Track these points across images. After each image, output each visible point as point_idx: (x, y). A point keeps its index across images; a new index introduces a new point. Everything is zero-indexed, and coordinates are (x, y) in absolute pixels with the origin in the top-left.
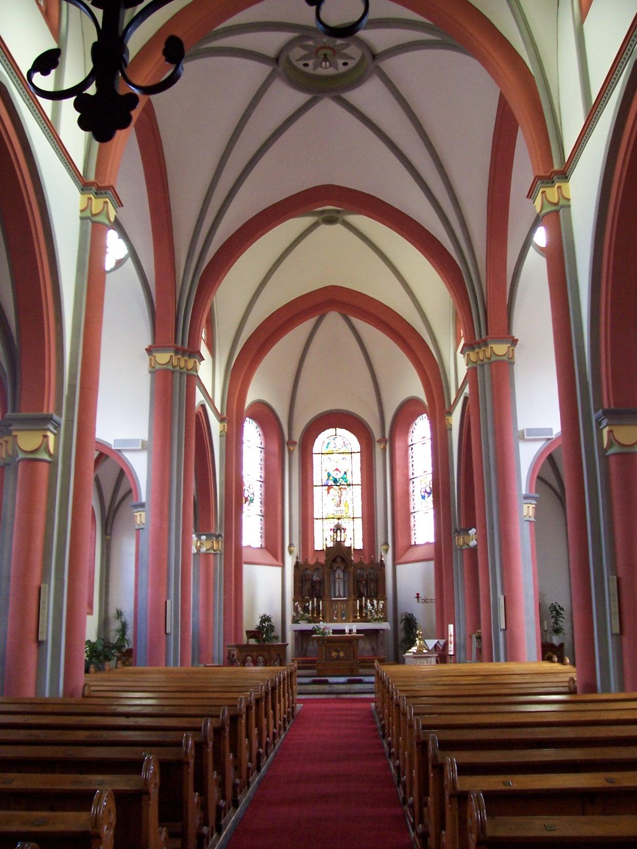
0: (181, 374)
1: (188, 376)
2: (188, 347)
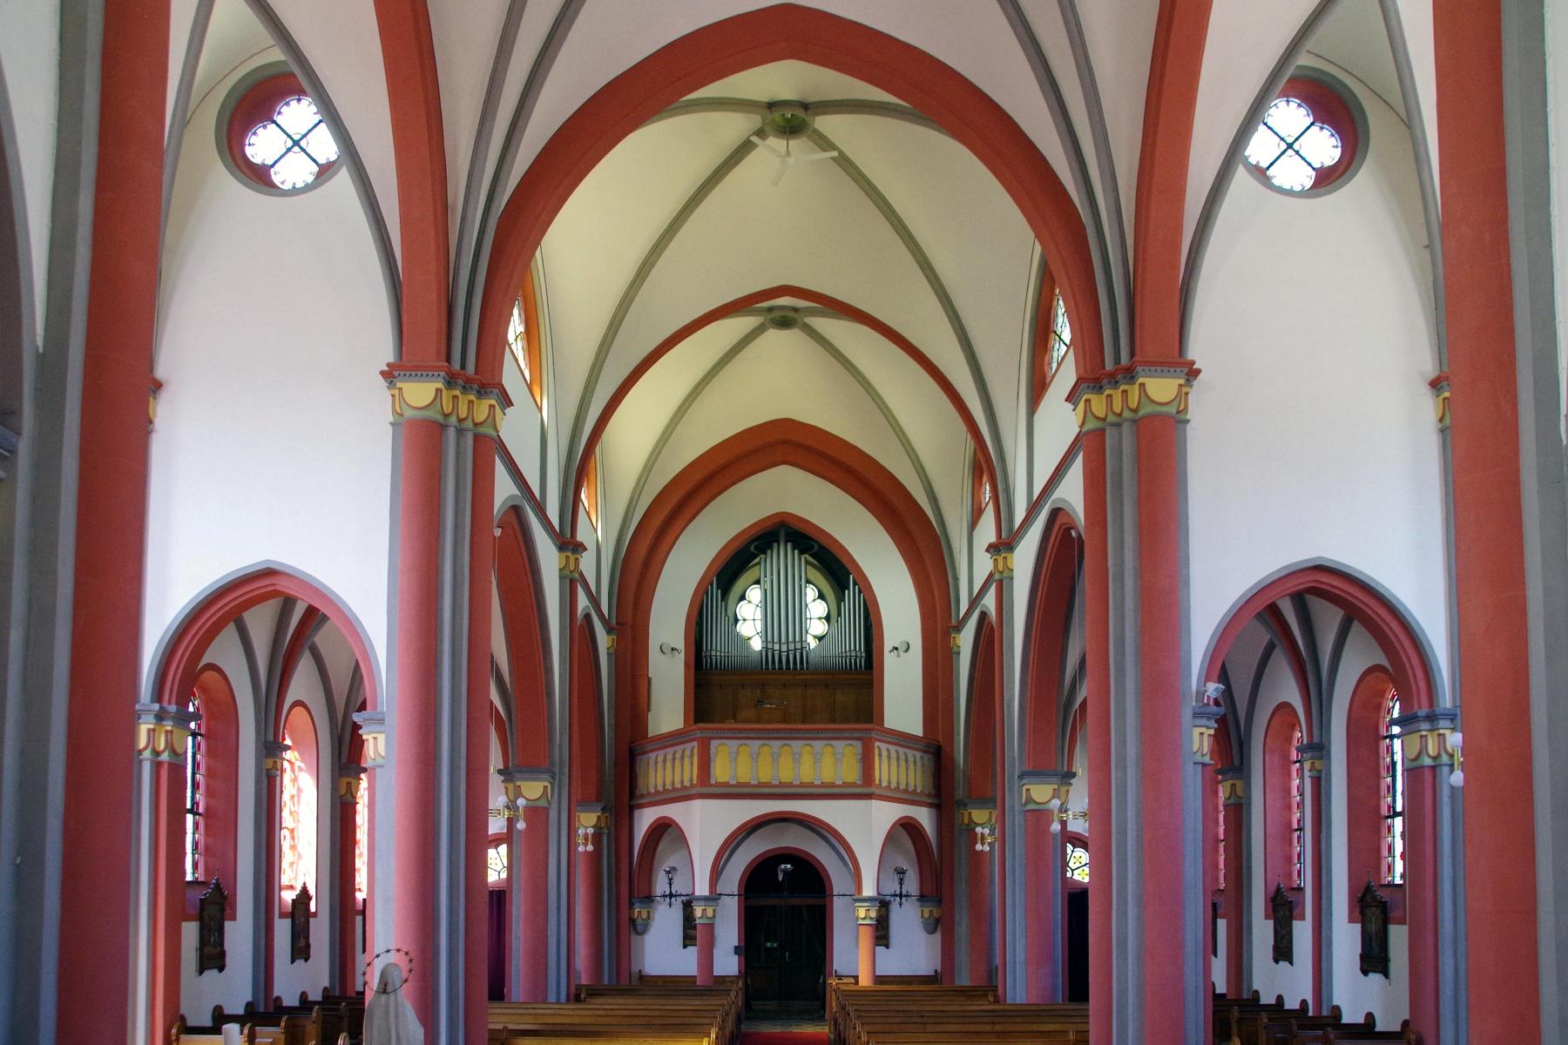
0: (460, 432)
1: (478, 438)
2: (476, 373)
